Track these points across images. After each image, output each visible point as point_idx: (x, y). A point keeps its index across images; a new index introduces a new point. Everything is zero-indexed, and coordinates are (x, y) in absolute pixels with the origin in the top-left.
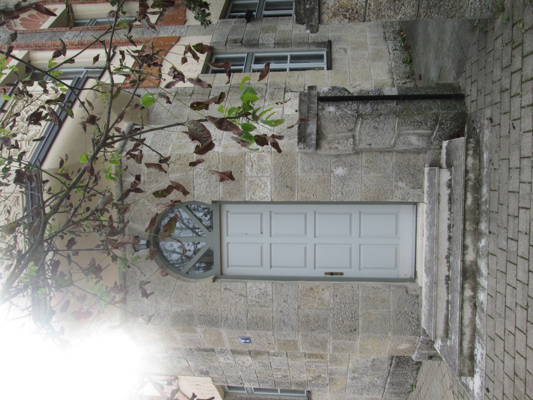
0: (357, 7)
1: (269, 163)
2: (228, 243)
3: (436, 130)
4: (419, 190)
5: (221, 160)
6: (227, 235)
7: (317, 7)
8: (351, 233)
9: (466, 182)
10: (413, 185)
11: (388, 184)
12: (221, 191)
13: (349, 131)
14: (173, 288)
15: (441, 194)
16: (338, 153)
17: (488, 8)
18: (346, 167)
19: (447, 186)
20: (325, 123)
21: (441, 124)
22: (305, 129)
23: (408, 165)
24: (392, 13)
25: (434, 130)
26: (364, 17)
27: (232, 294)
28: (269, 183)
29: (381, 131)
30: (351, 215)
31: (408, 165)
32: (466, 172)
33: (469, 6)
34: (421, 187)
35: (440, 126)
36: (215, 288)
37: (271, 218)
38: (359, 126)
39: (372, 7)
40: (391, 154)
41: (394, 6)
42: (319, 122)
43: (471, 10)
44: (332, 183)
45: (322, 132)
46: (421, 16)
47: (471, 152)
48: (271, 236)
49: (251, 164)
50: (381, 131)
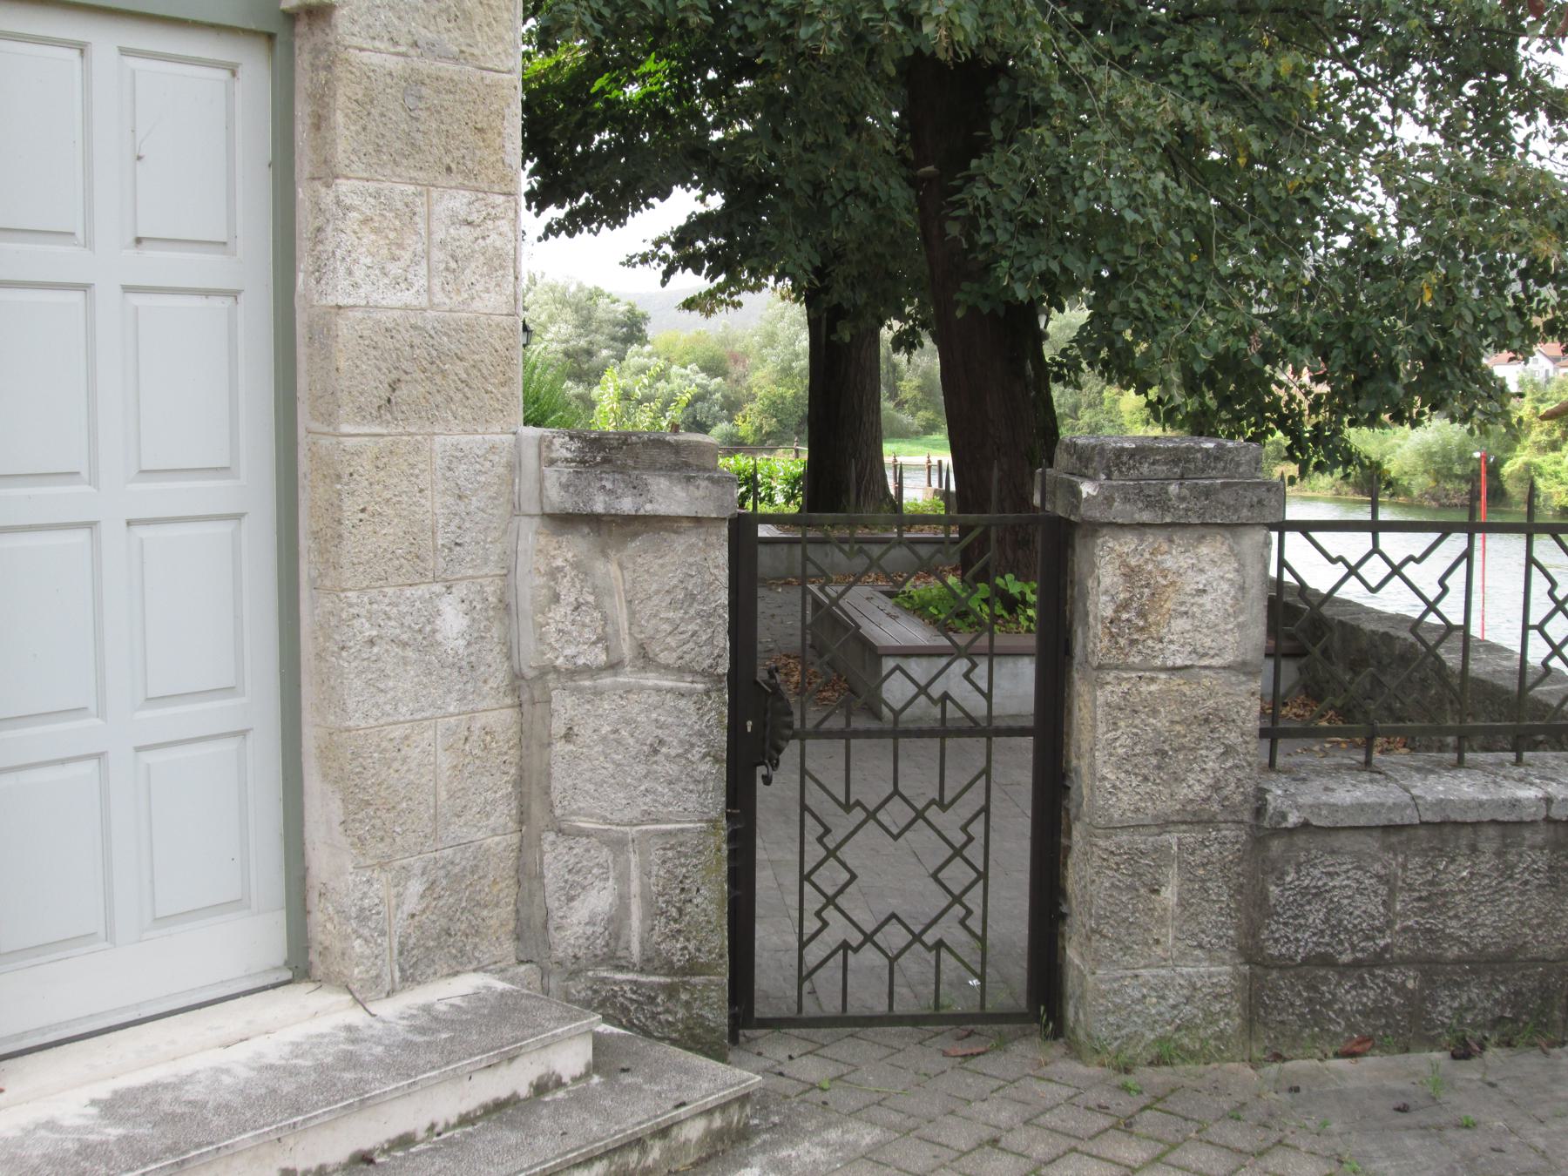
0: (1150, 642)
1: (477, 305)
2: (82, 48)
3: (643, 979)
4: (397, 974)
5: (490, 77)
6: (124, 52)
7: (1168, 520)
8: (151, 701)
9: (638, 1143)
10: (412, 941)
11: (412, 838)
12: (376, 59)
13: (642, 646)
15: (517, 1064)
16: (526, 605)
17: (1119, 1027)
18: (469, 644)
19: (540, 1078)
20: (680, 549)
21: (671, 991)
22: (653, 467)
23: (478, 904)
24: (1121, 751)
25: (642, 971)
26: (1117, 668)
28: (408, 297)
29: (641, 769)
30: (228, 691)
31: (478, 904)
32: (663, 1132)
33: (1129, 973)
34: (409, 978)
35: (663, 987)
37: (207, 293)
38: (667, 684)
39: (1144, 688)
40: (512, 825)
41: (1144, 754)
42: (685, 524)
43: (1116, 980)
44: (408, 592)
45: (635, 535)
46: (1108, 838)
47: (718, 1122)
48: (127, 289)
49: (474, 217)
50: (641, 769)
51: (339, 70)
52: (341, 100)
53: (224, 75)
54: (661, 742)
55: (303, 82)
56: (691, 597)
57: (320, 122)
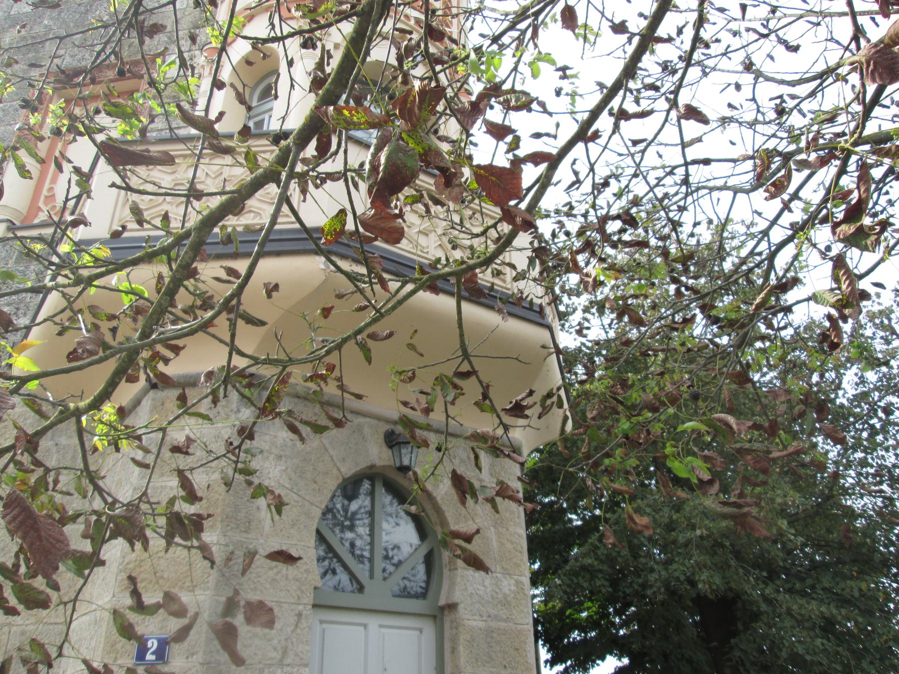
2: (365, 626)
5: (519, 627)
14: (307, 497)
27: (289, 629)
36: (302, 592)
51: (461, 629)
52: (462, 640)
53: (417, 633)
55: (447, 634)
57: (454, 650)
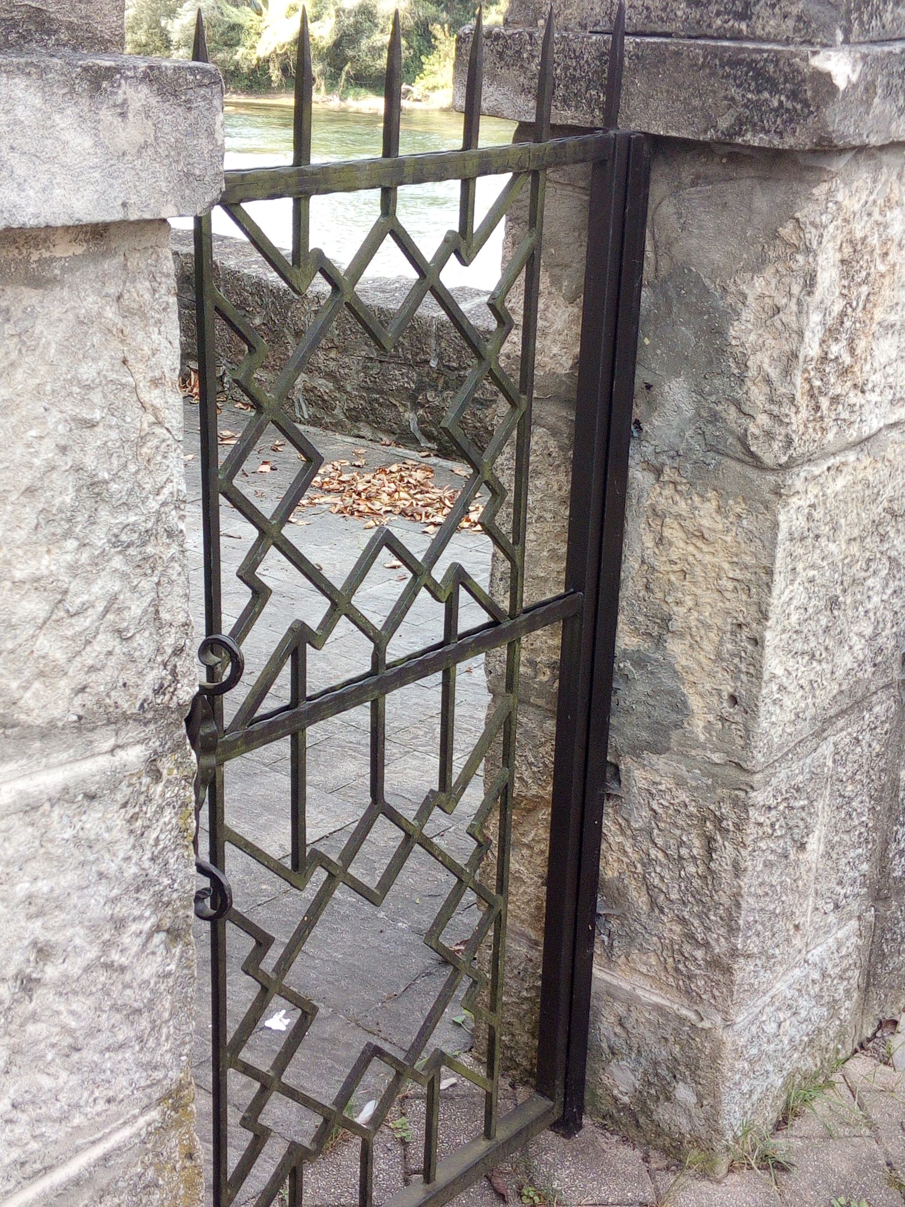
42: (63, 250)
54: (43, 952)
56: (94, 489)
